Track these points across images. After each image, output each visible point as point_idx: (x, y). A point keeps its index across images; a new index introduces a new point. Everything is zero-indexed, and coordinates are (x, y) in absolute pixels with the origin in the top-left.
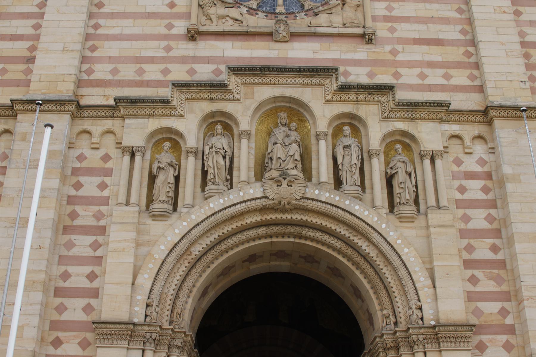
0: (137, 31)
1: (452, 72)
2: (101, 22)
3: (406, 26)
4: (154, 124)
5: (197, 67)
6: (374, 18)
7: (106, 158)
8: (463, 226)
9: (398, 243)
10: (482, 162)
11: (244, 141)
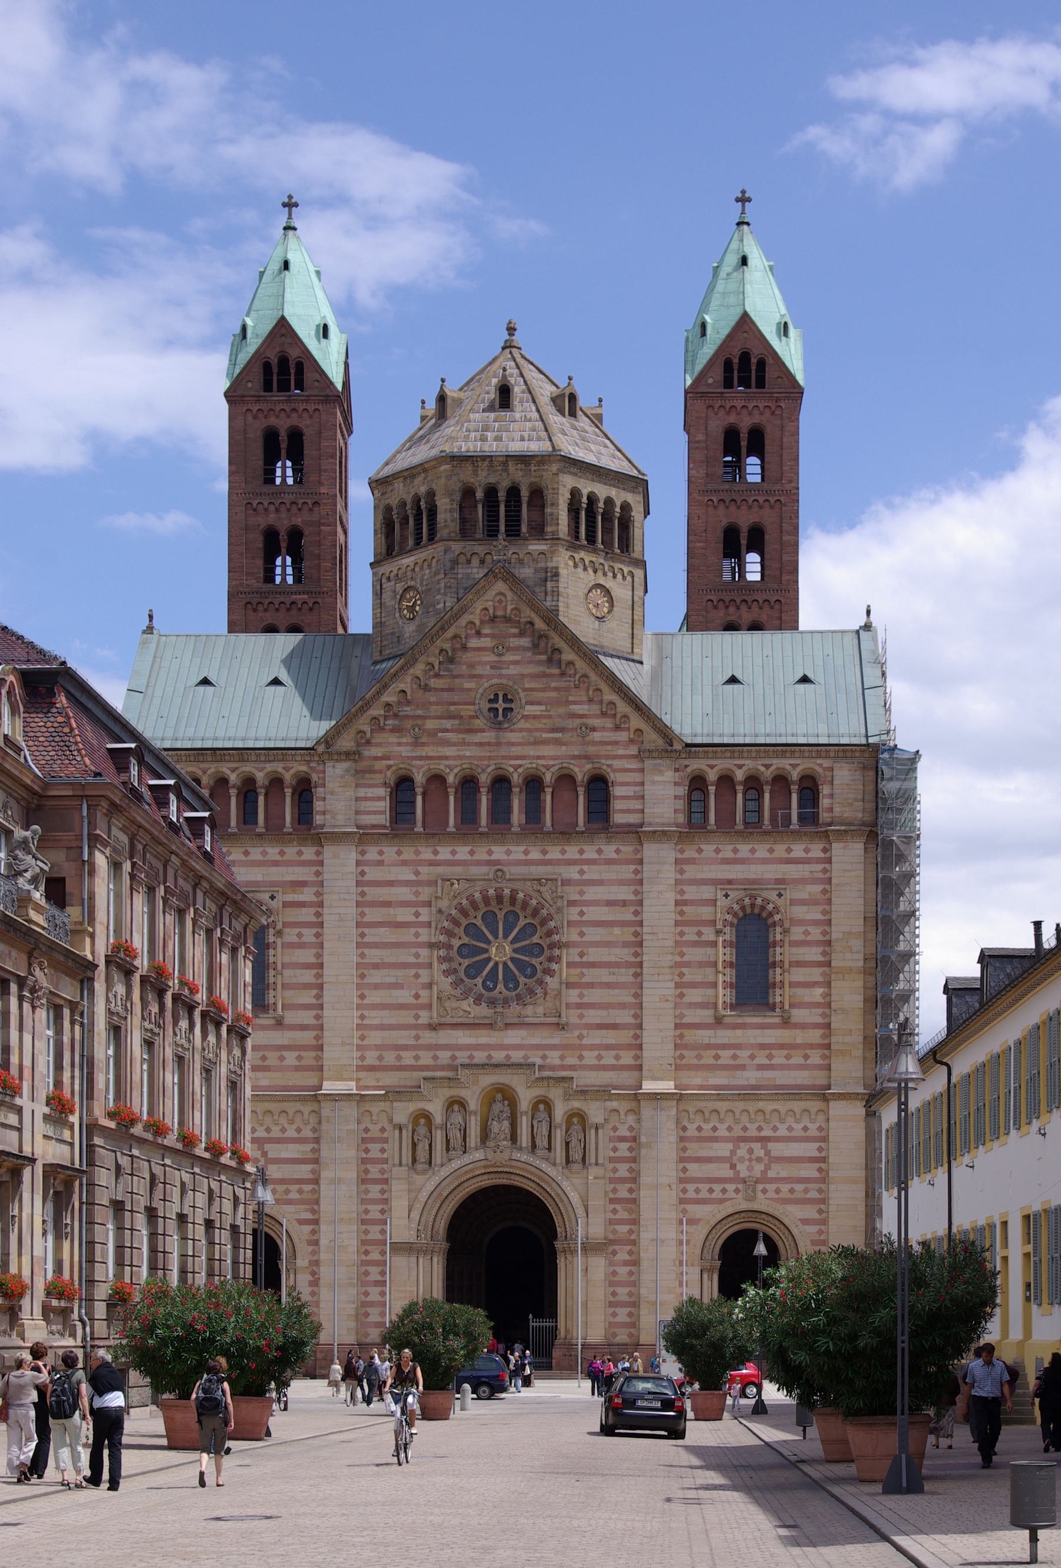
0: (393, 1021)
1: (621, 1053)
2: (366, 1013)
3: (592, 1012)
4: (413, 1107)
5: (440, 1053)
6: (568, 1006)
7: (383, 1130)
8: (612, 1175)
9: (568, 1189)
10: (631, 1129)
11: (473, 1118)
